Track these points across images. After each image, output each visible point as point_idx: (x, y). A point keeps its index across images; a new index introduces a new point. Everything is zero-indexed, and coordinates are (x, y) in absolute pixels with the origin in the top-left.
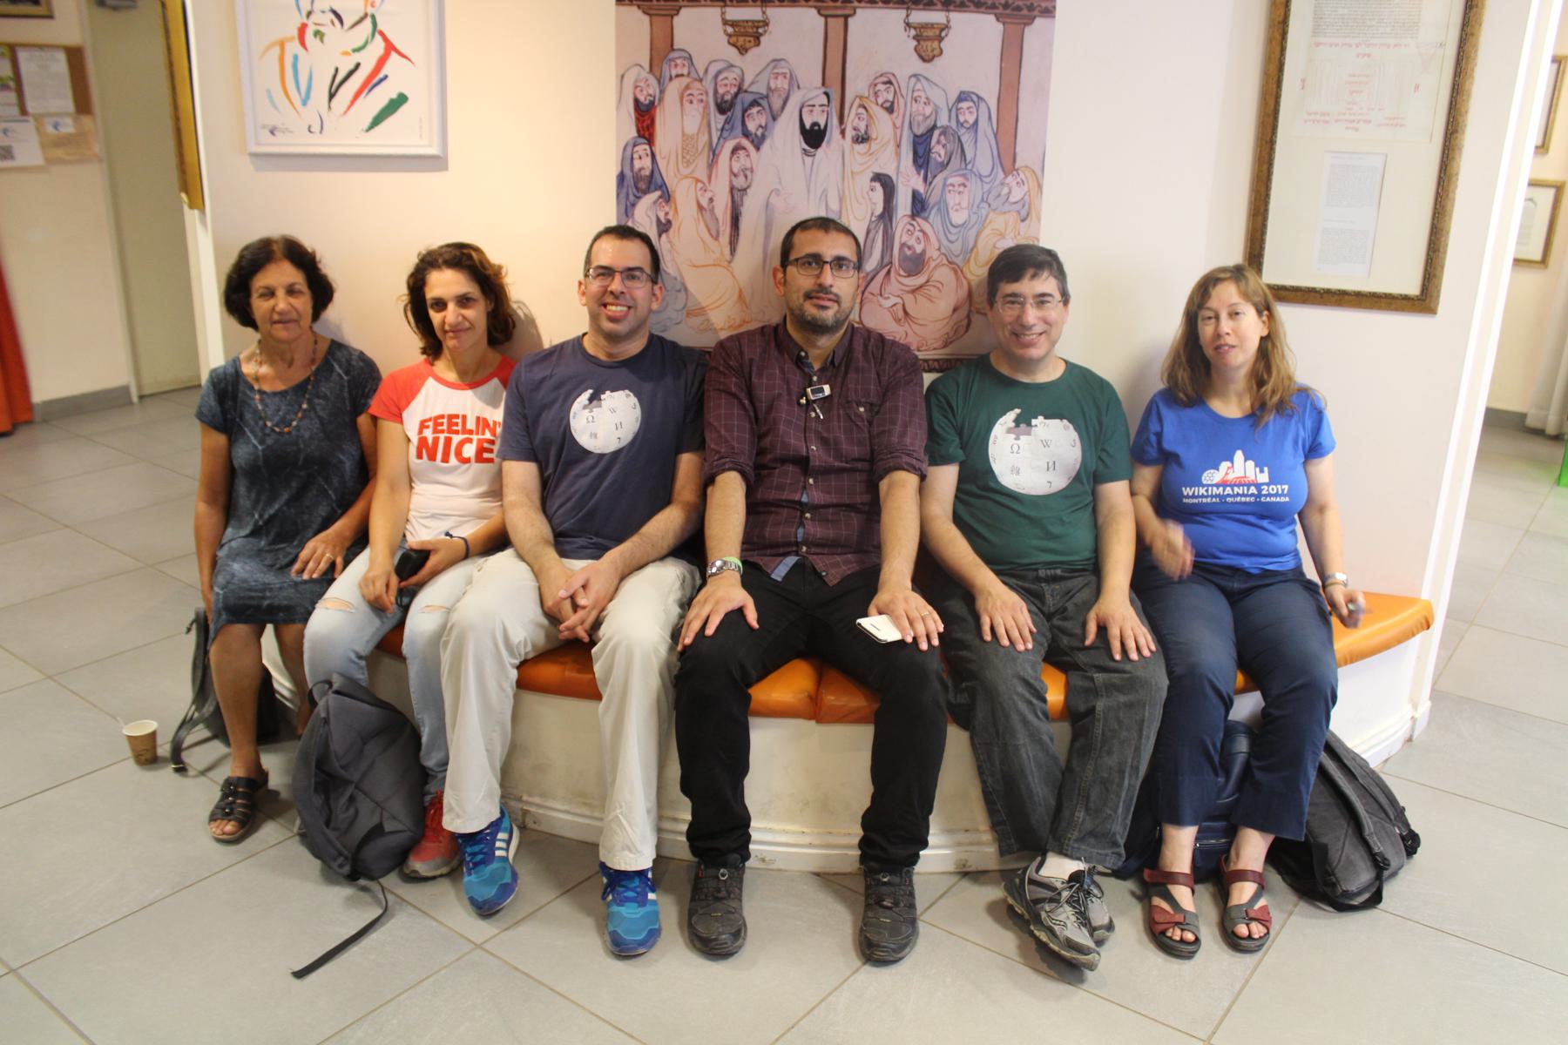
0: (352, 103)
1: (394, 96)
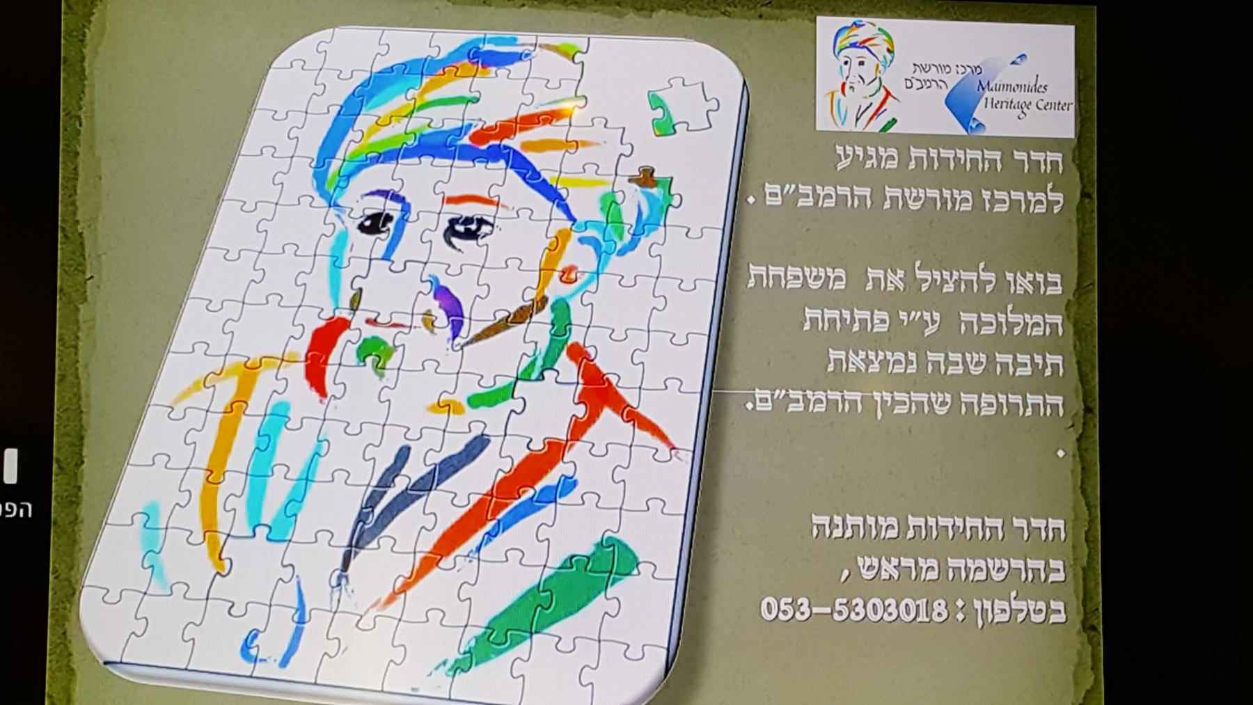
0: (428, 564)
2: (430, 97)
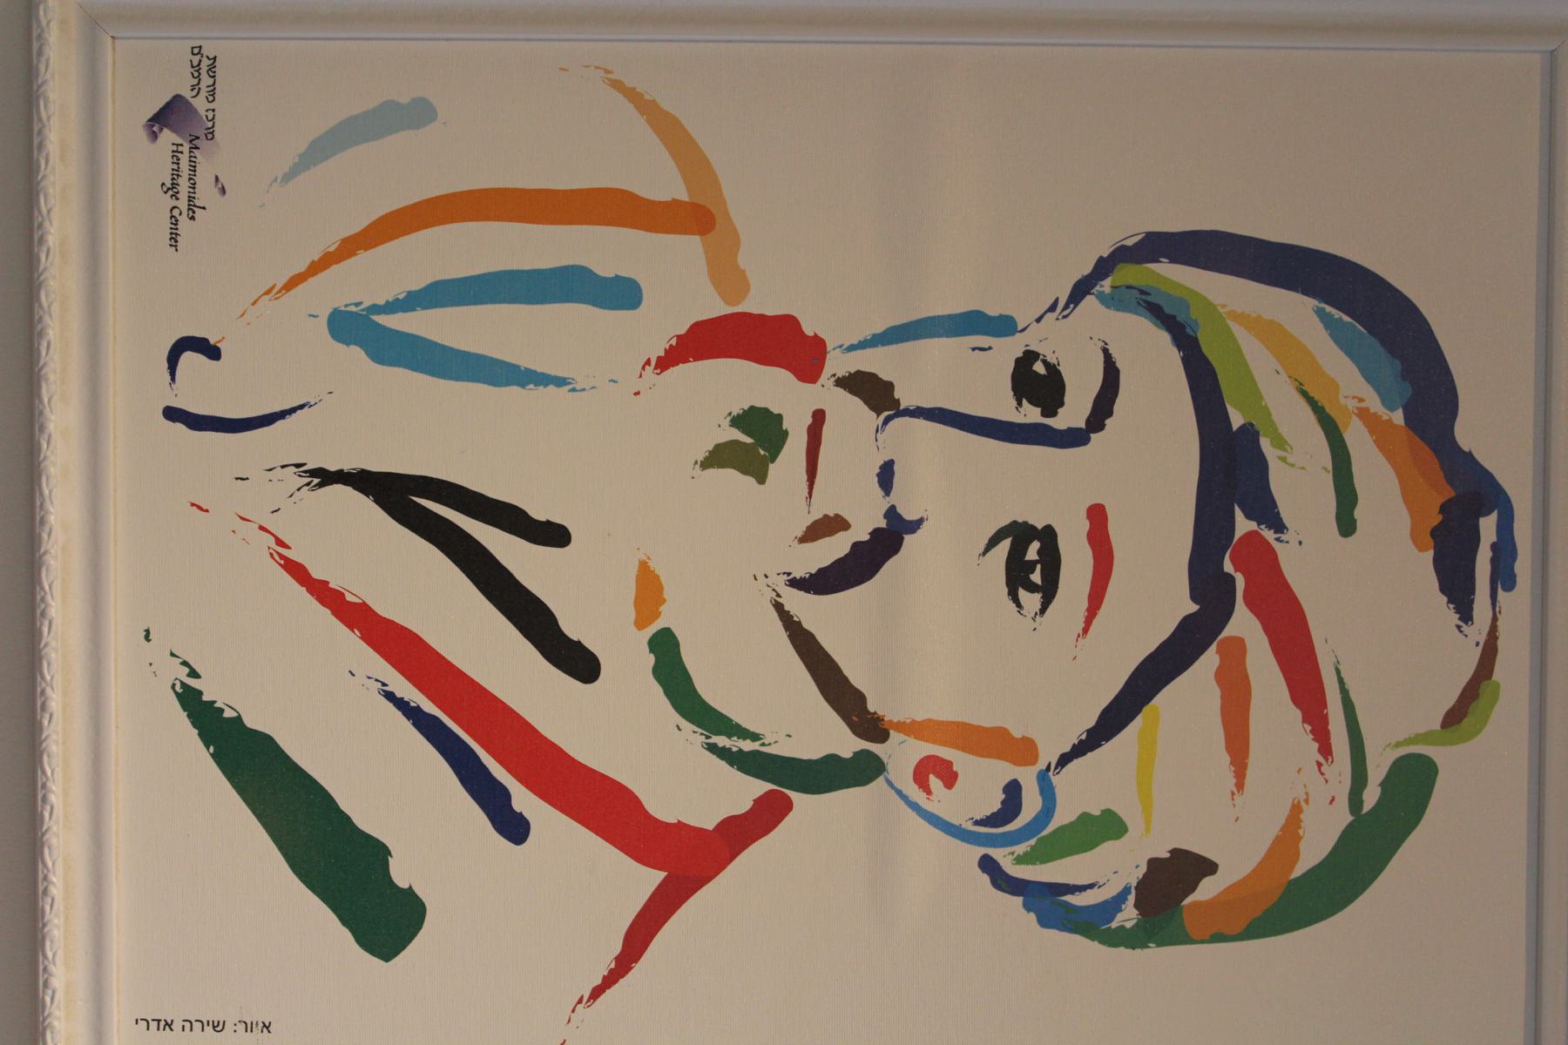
1: (401, 873)
2: (1357, 438)
